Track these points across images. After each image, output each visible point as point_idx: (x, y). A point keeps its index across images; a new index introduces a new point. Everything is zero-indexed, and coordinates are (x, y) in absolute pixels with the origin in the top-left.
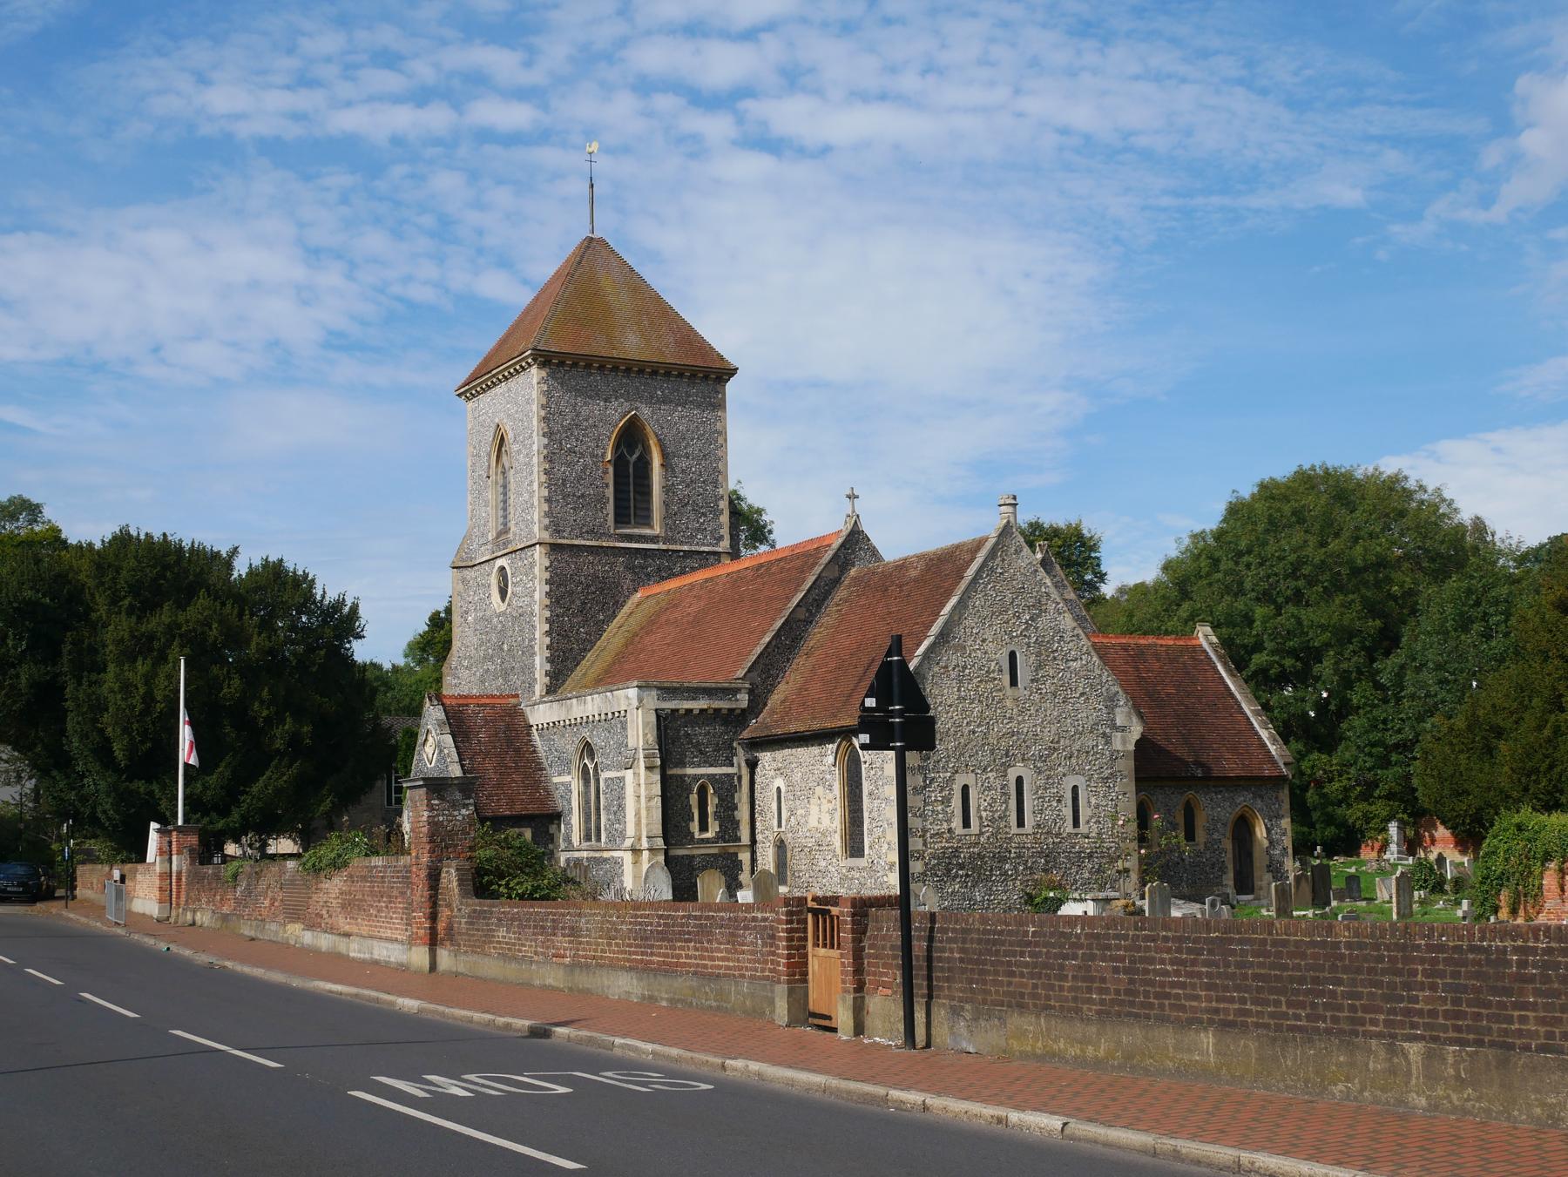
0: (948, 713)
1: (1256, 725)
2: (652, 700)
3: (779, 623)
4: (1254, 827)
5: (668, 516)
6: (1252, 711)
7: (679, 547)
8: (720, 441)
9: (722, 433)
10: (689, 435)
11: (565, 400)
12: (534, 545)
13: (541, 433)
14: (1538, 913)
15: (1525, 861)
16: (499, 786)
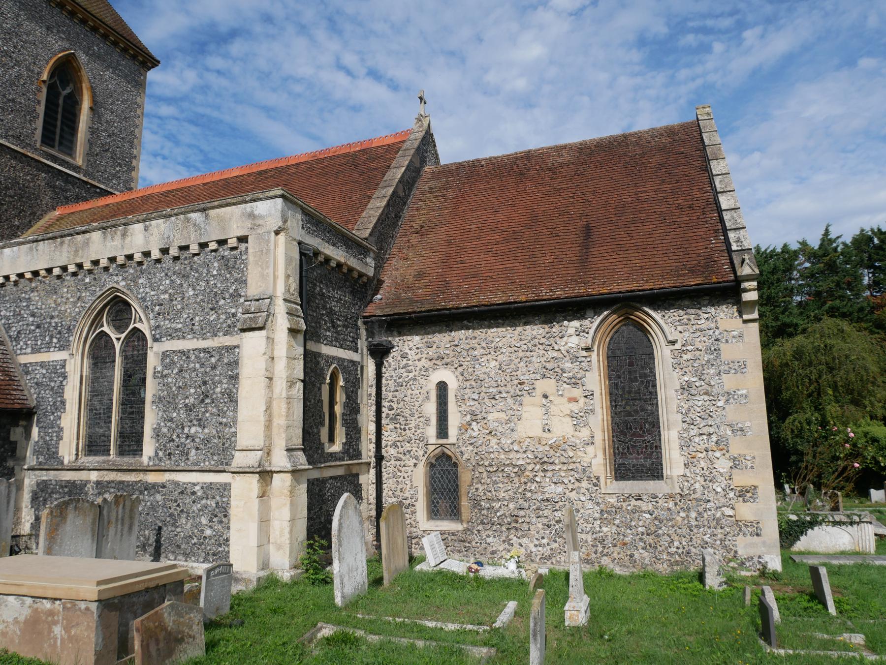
5: (89, 154)
7: (97, 184)
8: (139, 112)
10: (115, 95)
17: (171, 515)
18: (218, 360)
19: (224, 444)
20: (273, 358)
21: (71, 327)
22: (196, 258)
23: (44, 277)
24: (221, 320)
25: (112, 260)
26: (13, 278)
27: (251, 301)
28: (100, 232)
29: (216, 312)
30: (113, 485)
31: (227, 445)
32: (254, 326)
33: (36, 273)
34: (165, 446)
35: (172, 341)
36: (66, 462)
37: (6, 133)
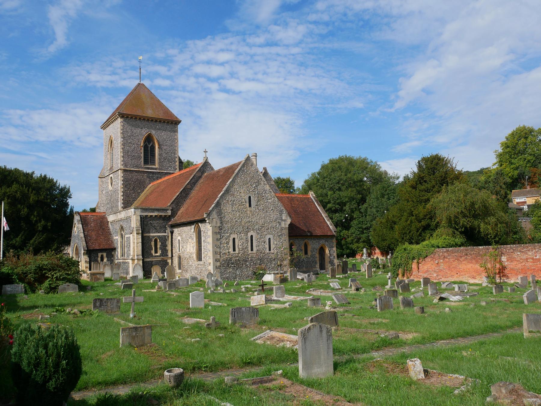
0: (228, 215)
1: (326, 220)
2: (139, 212)
3: (182, 189)
4: (325, 250)
5: (160, 162)
6: (325, 216)
7: (163, 171)
8: (176, 141)
9: (177, 139)
11: (129, 128)
12: (119, 170)
13: (121, 137)
14: (411, 276)
15: (407, 260)
16: (96, 240)
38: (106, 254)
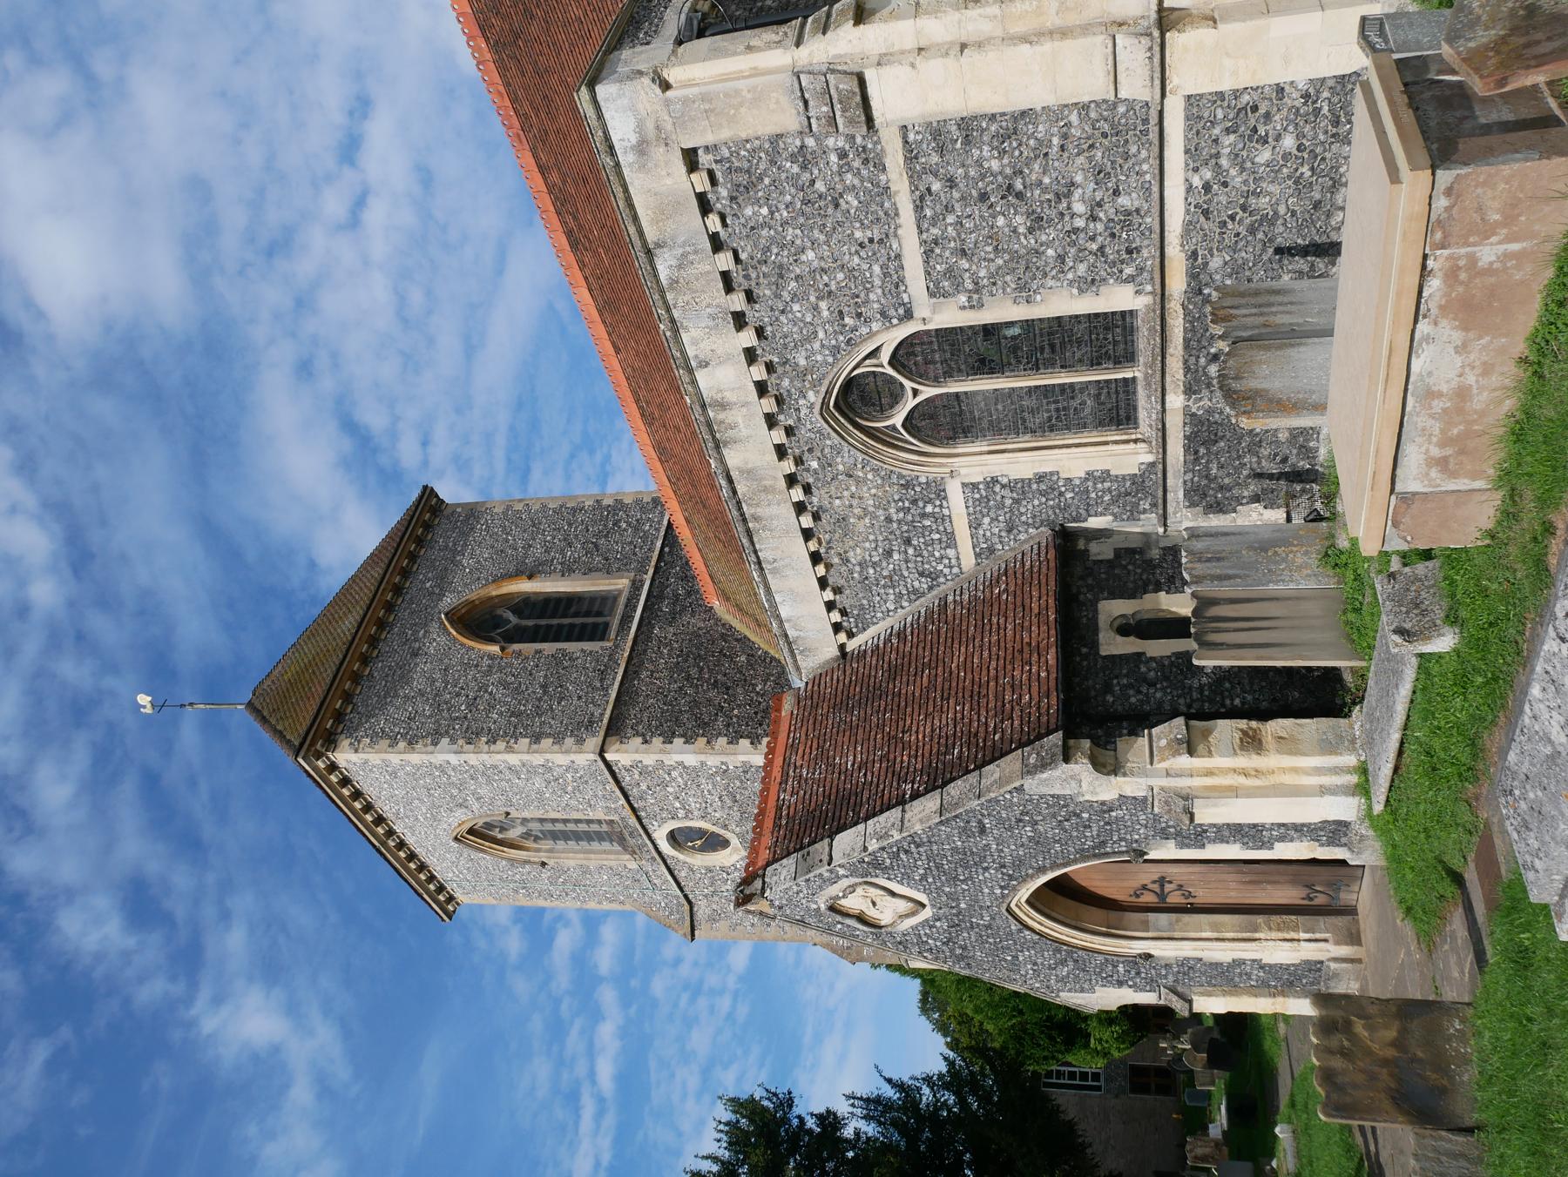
8: (519, 507)
10: (499, 546)
11: (397, 711)
13: (431, 748)
16: (976, 696)
17: (1252, 230)
18: (936, 176)
19: (1105, 135)
20: (920, 49)
21: (902, 482)
22: (743, 256)
23: (820, 543)
24: (856, 182)
25: (771, 421)
26: (829, 595)
27: (809, 118)
28: (725, 452)
29: (841, 195)
30: (1192, 360)
31: (1106, 127)
32: (858, 98)
33: (816, 558)
34: (1114, 263)
35: (908, 281)
36: (1150, 458)
37: (598, 689)
38: (1113, 596)
